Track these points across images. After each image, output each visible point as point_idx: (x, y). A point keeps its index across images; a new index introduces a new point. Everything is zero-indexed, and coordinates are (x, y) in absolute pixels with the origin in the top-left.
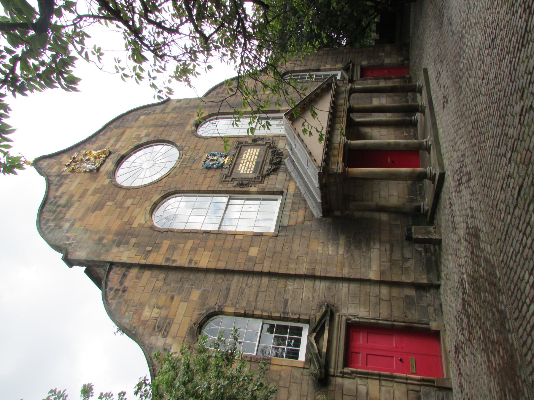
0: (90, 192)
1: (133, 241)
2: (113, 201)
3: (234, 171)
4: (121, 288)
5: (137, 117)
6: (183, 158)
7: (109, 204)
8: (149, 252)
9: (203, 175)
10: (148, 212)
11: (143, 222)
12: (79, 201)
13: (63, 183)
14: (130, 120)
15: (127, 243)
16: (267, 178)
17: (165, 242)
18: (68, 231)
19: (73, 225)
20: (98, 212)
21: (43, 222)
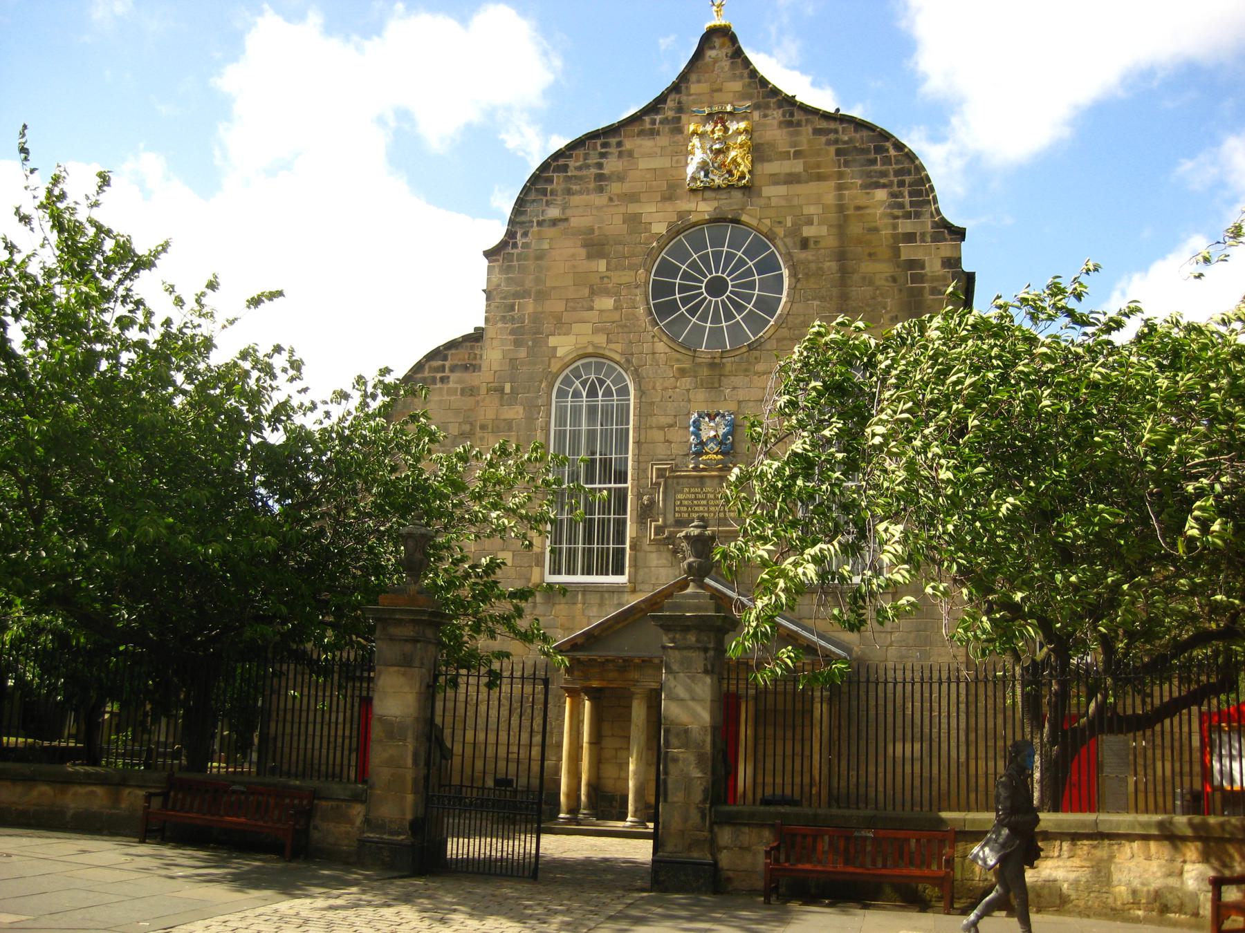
0: (633, 208)
1: (522, 353)
2: (608, 270)
3: (681, 481)
4: (447, 373)
5: (882, 181)
6: (724, 360)
7: (602, 265)
8: (502, 390)
9: (670, 420)
10: (580, 352)
11: (560, 352)
12: (611, 199)
13: (658, 133)
14: (872, 168)
15: (518, 344)
16: (662, 548)
17: (520, 409)
18: (540, 224)
19: (554, 222)
20: (583, 252)
21: (561, 162)
